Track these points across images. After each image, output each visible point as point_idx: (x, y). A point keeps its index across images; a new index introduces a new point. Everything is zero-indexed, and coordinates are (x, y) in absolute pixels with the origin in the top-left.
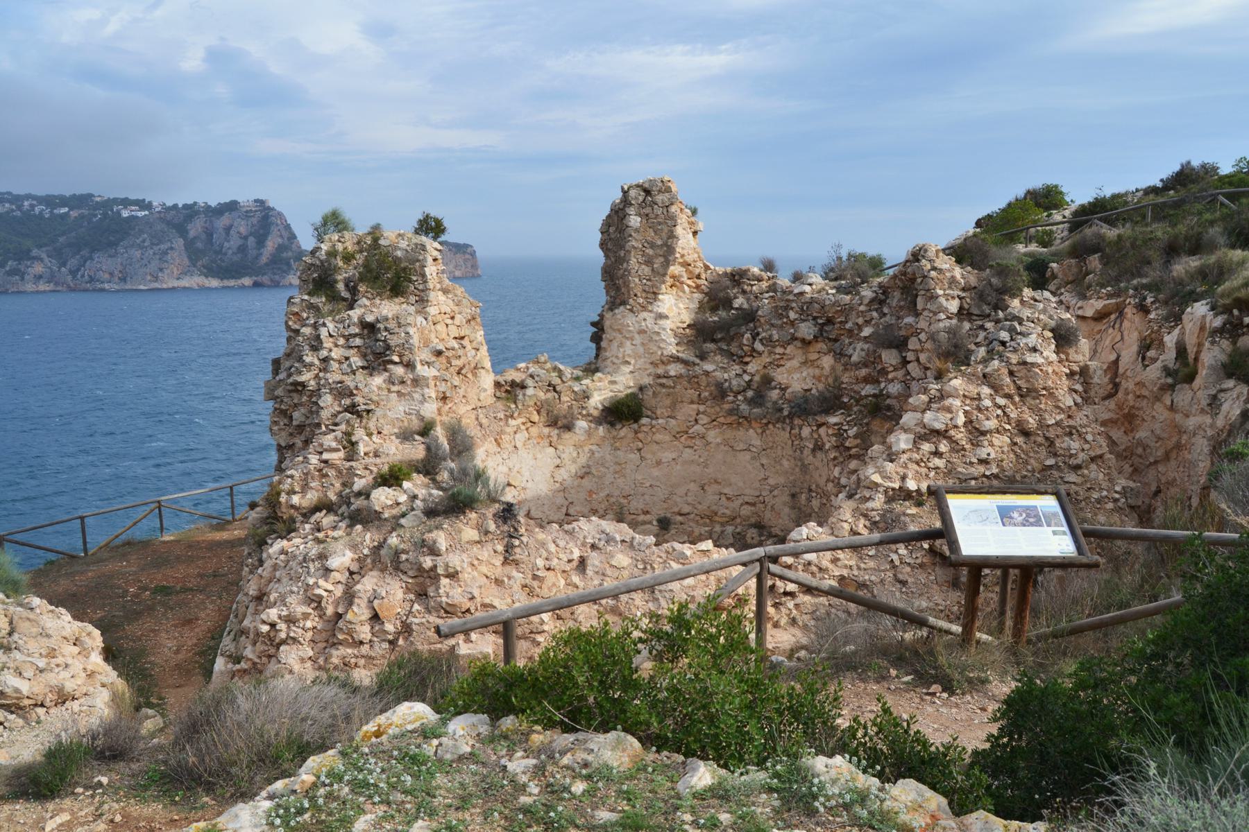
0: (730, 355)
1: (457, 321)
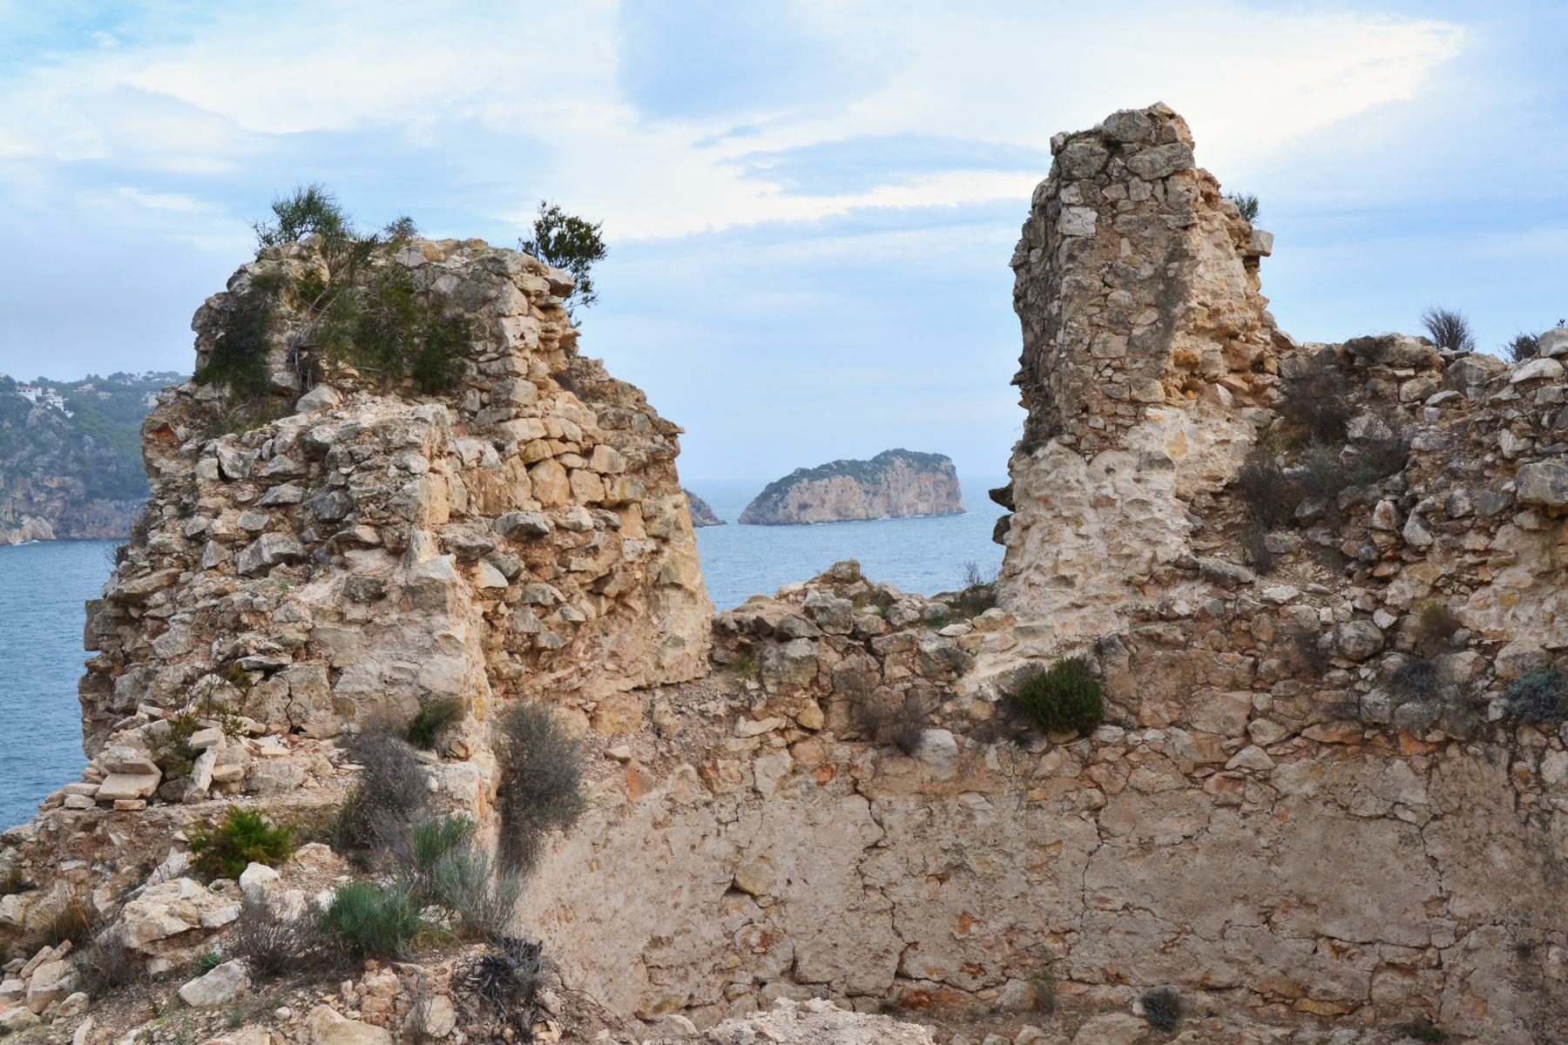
0: (1338, 560)
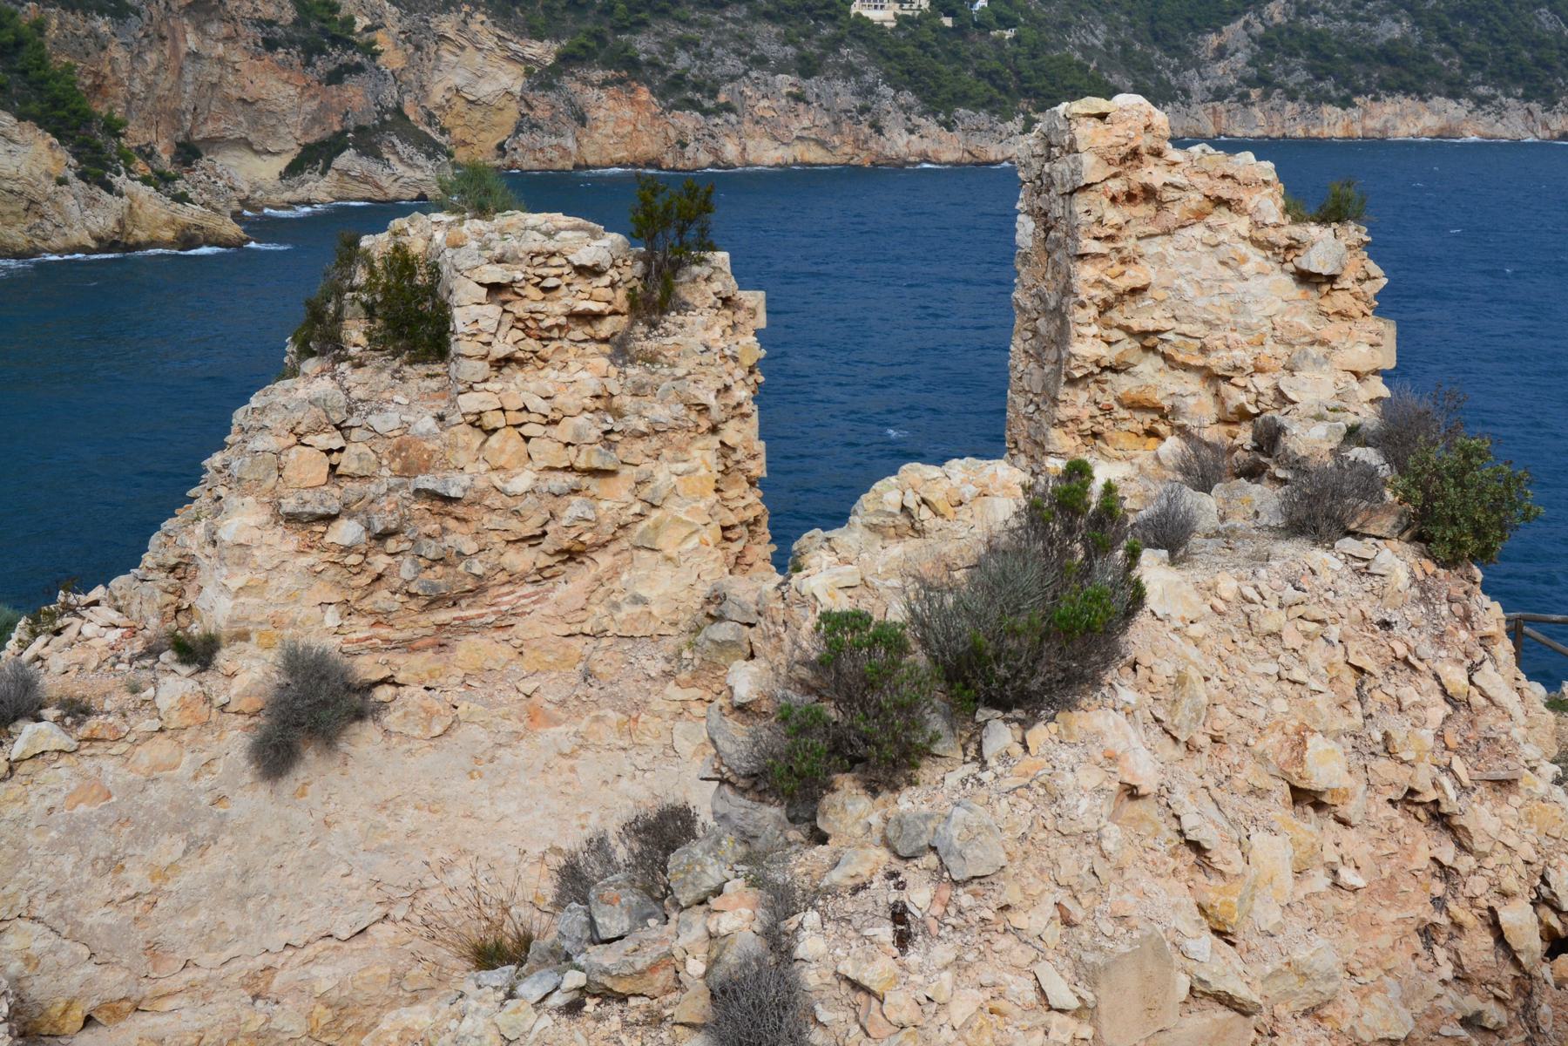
1: (564, 431)
